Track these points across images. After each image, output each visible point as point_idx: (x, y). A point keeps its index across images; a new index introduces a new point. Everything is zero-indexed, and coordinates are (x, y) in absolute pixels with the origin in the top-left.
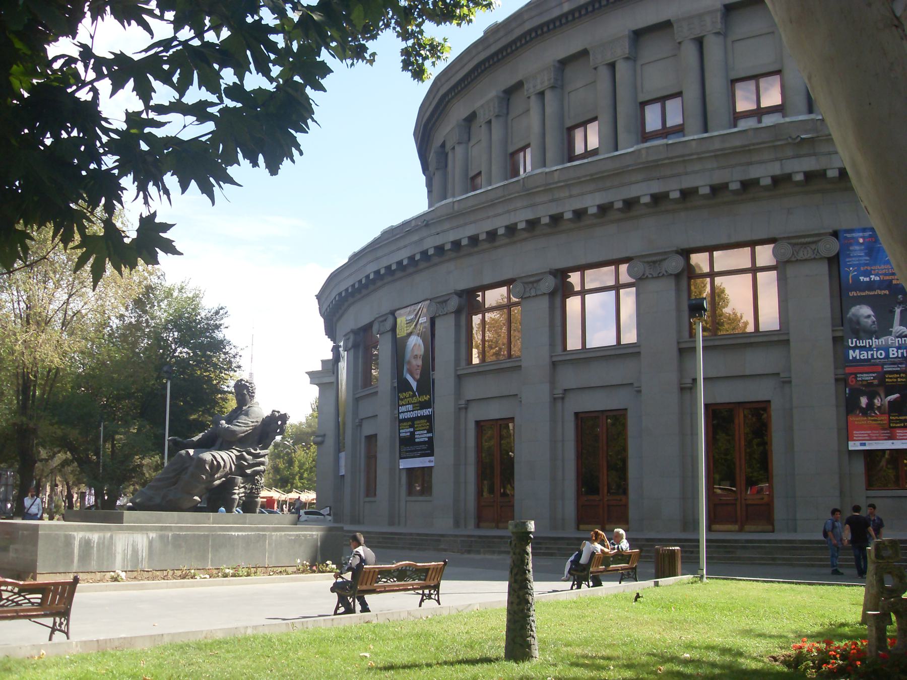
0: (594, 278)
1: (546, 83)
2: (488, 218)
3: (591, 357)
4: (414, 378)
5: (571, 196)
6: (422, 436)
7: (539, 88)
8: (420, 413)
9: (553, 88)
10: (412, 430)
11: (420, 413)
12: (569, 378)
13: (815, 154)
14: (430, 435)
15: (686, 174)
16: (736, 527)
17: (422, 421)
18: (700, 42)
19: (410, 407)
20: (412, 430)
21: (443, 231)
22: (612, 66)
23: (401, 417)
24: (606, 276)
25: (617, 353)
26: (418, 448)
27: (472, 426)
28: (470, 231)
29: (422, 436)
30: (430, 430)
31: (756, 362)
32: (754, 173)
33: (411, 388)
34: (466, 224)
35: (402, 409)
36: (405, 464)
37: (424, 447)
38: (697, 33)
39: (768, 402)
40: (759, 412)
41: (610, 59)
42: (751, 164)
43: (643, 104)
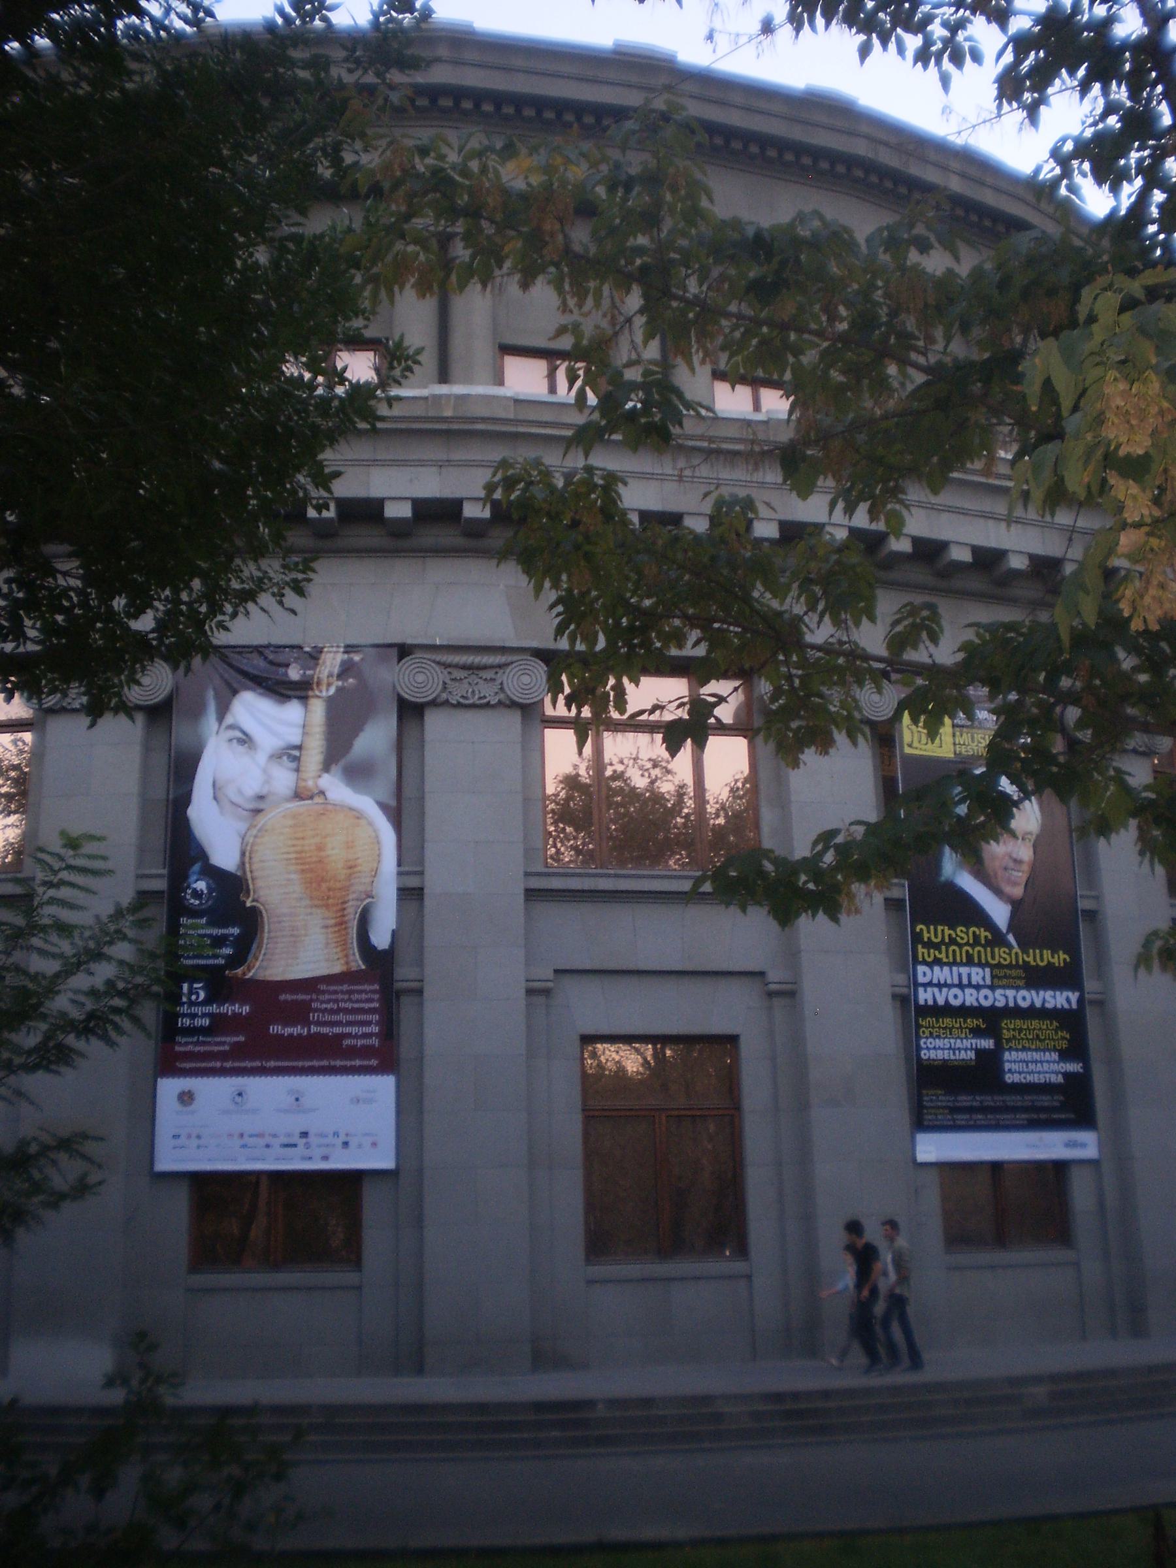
4: (998, 892)
6: (1032, 1064)
8: (1026, 998)
10: (987, 1044)
11: (1026, 998)
14: (1074, 1067)
17: (1035, 1023)
19: (978, 975)
20: (987, 1044)
23: (925, 996)
26: (1012, 1100)
29: (1032, 1064)
30: (1076, 1049)
33: (983, 919)
35: (923, 973)
37: (1045, 1100)
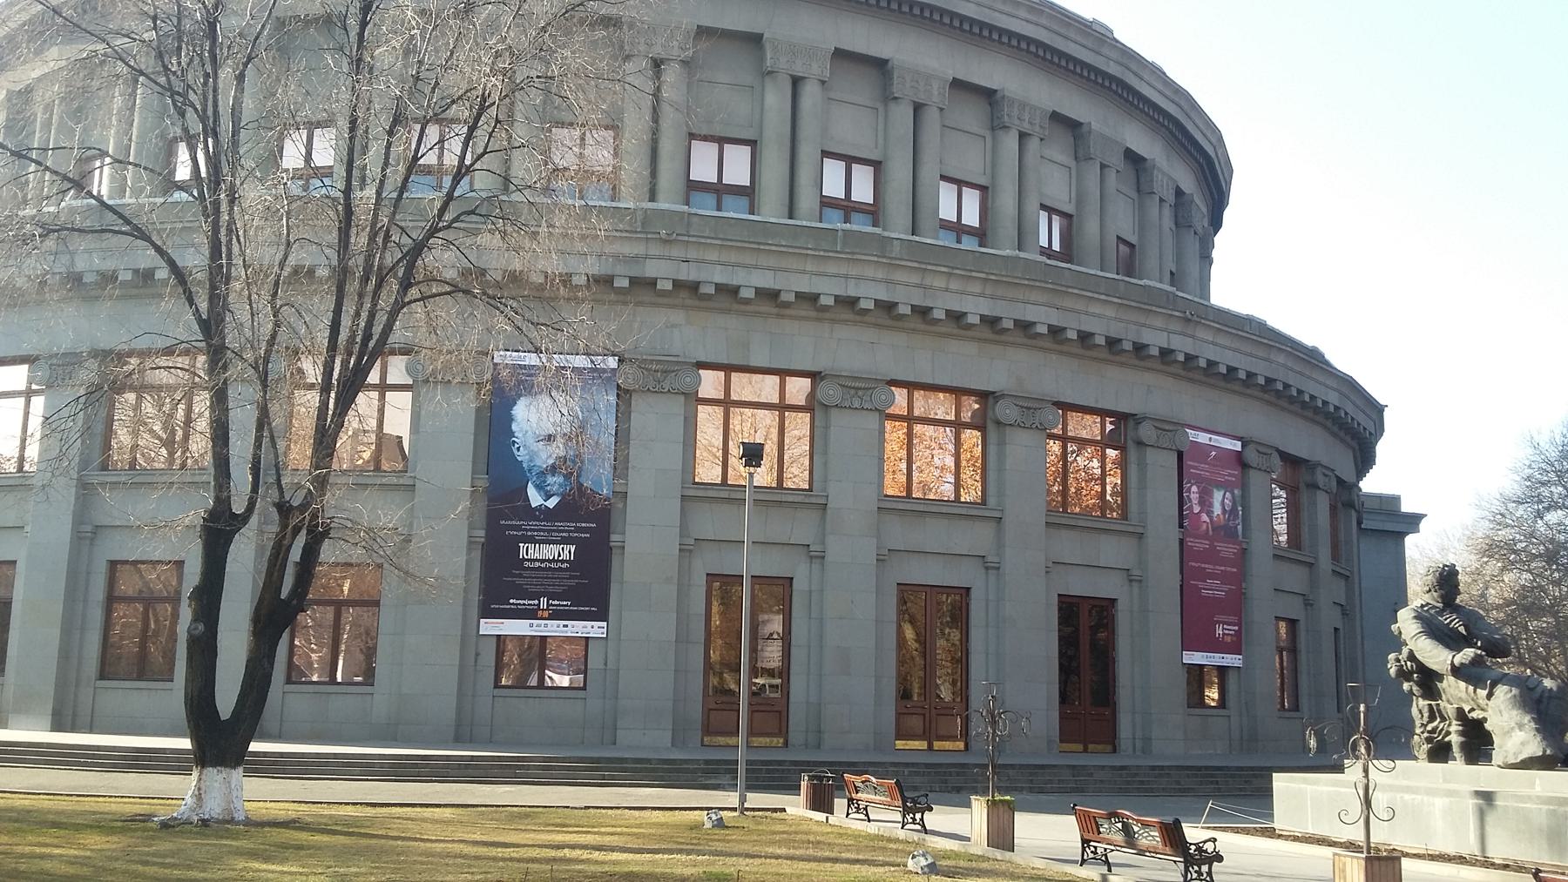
0: (925, 404)
1: (676, 52)
2: (804, 272)
3: (911, 507)
5: (947, 290)
7: (658, 51)
9: (685, 63)
12: (900, 534)
13: (1193, 337)
15: (1087, 313)
16: (1080, 747)
18: (918, 108)
21: (703, 261)
22: (796, 82)
24: (942, 406)
25: (952, 511)
27: (700, 581)
28: (766, 281)
31: (1112, 551)
32: (1147, 337)
34: (756, 267)
36: (490, 627)
38: (921, 98)
39: (1113, 601)
40: (1104, 610)
41: (799, 70)
42: (1144, 325)
43: (826, 154)
